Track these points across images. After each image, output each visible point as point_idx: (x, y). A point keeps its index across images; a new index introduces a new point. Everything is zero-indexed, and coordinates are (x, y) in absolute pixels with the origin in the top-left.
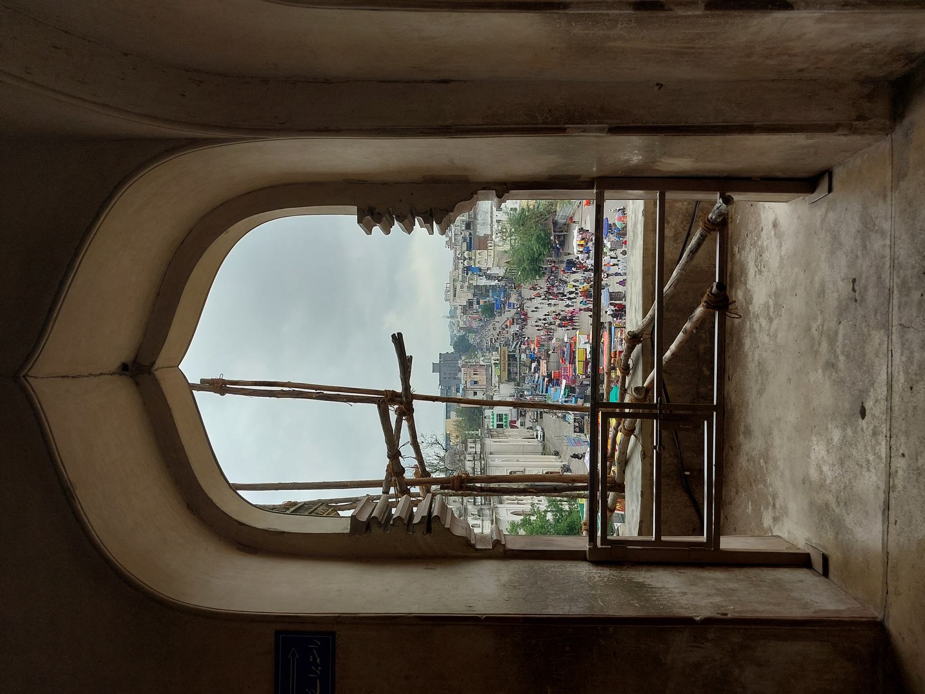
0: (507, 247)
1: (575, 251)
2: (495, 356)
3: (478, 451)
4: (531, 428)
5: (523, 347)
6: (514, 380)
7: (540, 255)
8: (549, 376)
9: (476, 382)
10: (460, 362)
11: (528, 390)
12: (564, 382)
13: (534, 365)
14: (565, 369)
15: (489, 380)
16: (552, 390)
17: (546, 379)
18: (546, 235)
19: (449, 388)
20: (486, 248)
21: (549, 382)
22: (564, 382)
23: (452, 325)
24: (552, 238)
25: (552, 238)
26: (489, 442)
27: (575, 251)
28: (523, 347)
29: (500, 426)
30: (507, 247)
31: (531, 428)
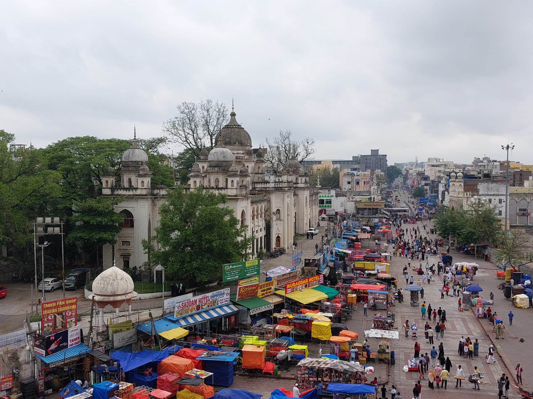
0: (466, 208)
1: (458, 264)
2: (378, 198)
3: (299, 185)
4: (319, 225)
5: (384, 220)
6: (358, 213)
7: (459, 235)
8: (357, 240)
9: (358, 183)
10: (379, 171)
11: (347, 223)
12: (349, 252)
13: (368, 228)
14: (360, 253)
15: (359, 194)
16: (345, 242)
17: (354, 238)
18: (475, 239)
19: (359, 163)
20: (465, 190)
21: (352, 240)
22: (349, 252)
23: (411, 164)
24: (472, 245)
25: (472, 245)
26: (307, 193)
27: (458, 264)
28: (384, 220)
29: (322, 202)
30: (466, 208)
31: (319, 225)
